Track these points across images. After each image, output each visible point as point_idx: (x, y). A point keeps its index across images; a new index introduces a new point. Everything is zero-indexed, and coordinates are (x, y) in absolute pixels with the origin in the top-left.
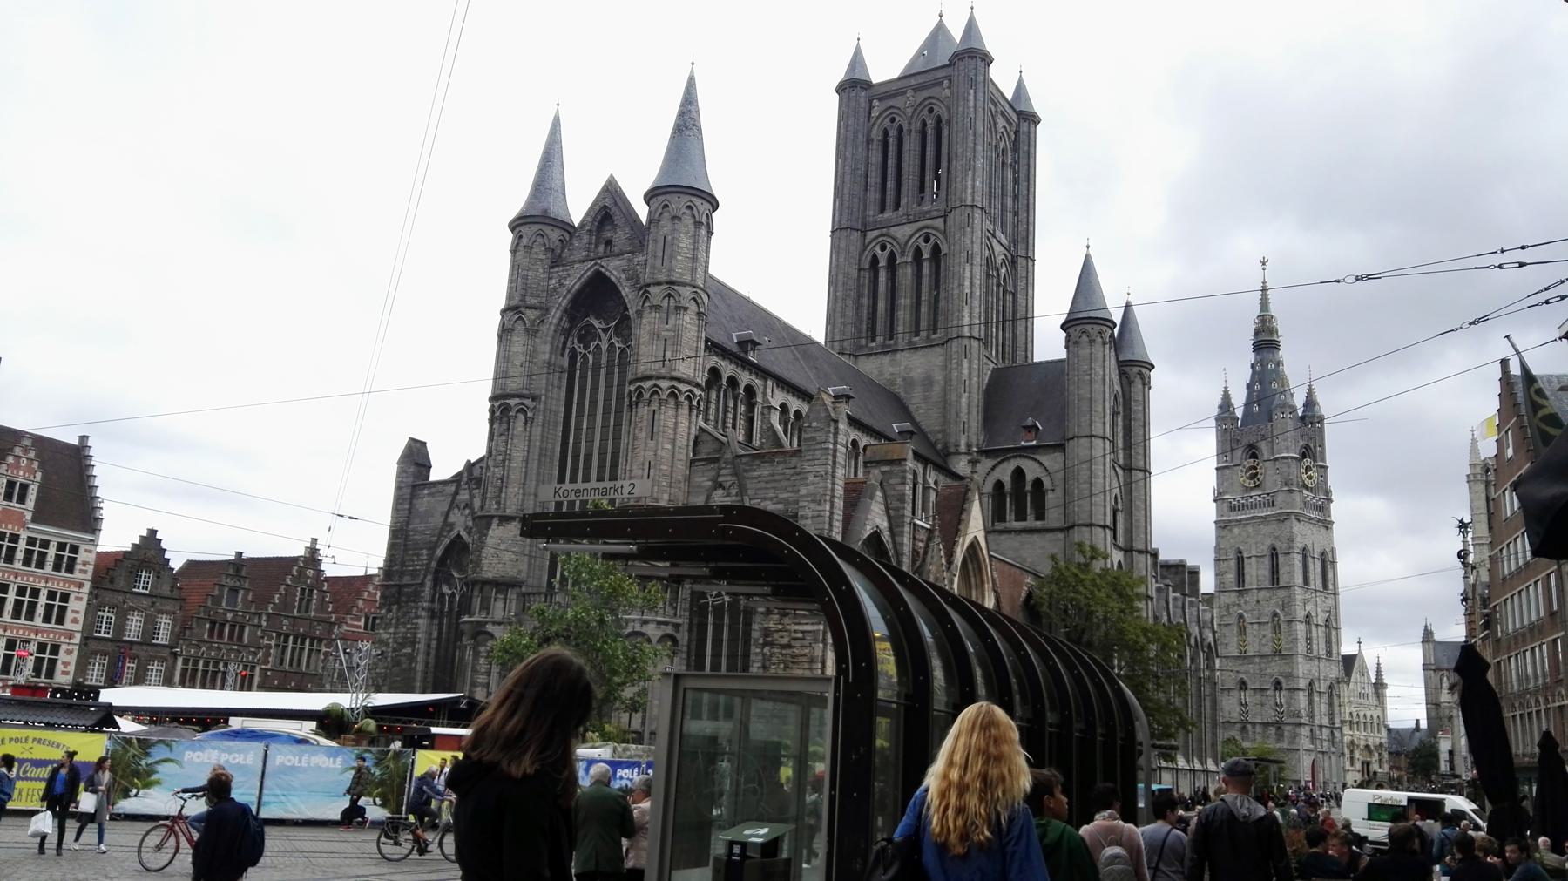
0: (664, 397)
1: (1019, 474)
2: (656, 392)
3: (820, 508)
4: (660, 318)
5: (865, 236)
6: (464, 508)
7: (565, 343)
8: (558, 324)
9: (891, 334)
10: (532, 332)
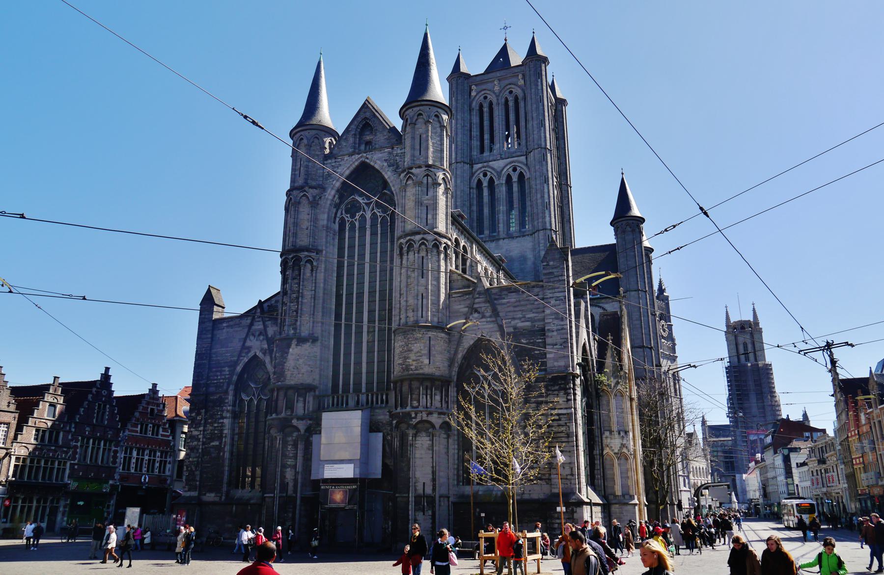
0: (431, 247)
2: (423, 243)
3: (562, 323)
4: (422, 191)
5: (472, 167)
6: (259, 335)
7: (336, 214)
8: (332, 200)
9: (494, 227)
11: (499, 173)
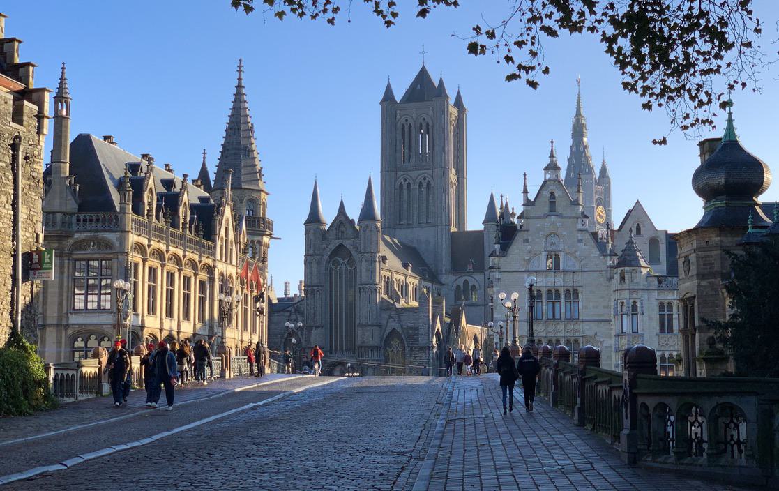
1: (466, 281)
10: (319, 263)
11: (414, 180)
